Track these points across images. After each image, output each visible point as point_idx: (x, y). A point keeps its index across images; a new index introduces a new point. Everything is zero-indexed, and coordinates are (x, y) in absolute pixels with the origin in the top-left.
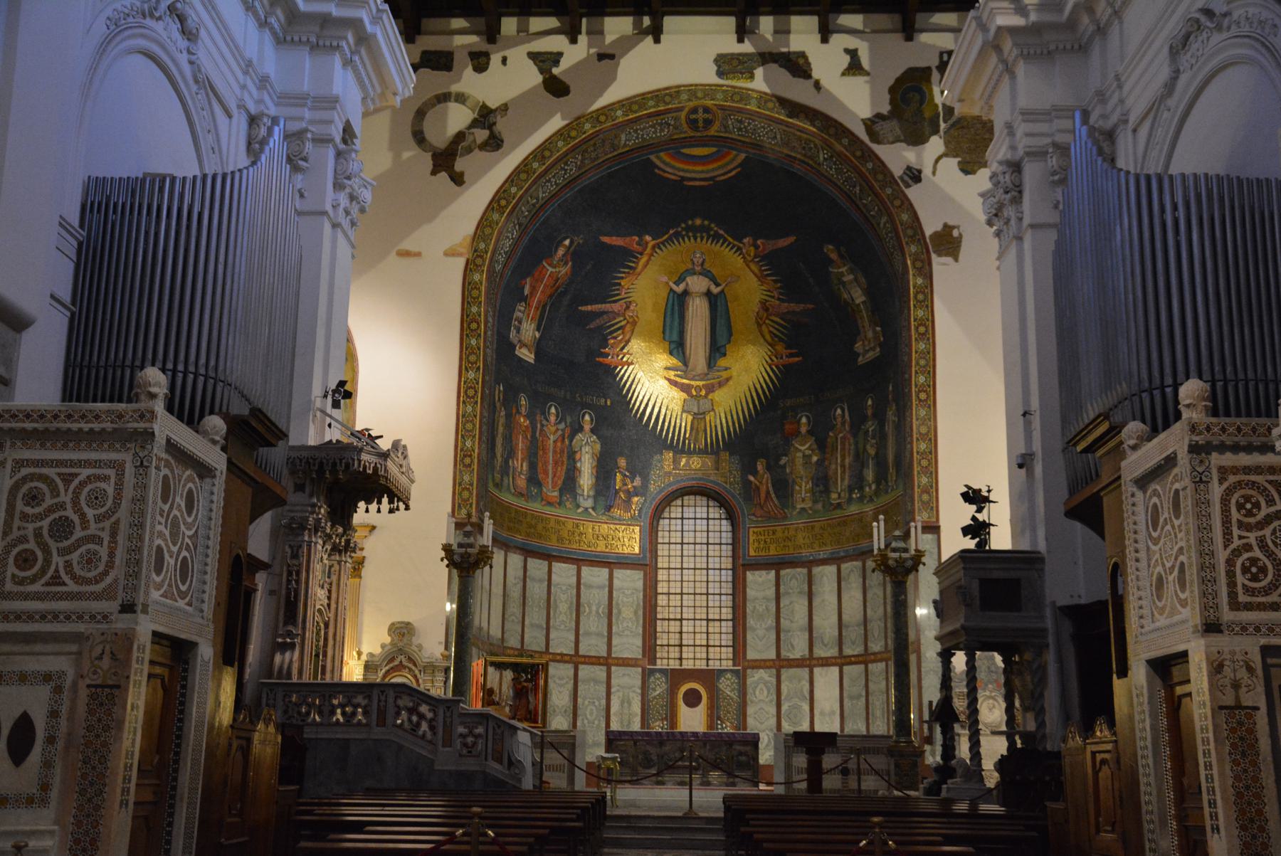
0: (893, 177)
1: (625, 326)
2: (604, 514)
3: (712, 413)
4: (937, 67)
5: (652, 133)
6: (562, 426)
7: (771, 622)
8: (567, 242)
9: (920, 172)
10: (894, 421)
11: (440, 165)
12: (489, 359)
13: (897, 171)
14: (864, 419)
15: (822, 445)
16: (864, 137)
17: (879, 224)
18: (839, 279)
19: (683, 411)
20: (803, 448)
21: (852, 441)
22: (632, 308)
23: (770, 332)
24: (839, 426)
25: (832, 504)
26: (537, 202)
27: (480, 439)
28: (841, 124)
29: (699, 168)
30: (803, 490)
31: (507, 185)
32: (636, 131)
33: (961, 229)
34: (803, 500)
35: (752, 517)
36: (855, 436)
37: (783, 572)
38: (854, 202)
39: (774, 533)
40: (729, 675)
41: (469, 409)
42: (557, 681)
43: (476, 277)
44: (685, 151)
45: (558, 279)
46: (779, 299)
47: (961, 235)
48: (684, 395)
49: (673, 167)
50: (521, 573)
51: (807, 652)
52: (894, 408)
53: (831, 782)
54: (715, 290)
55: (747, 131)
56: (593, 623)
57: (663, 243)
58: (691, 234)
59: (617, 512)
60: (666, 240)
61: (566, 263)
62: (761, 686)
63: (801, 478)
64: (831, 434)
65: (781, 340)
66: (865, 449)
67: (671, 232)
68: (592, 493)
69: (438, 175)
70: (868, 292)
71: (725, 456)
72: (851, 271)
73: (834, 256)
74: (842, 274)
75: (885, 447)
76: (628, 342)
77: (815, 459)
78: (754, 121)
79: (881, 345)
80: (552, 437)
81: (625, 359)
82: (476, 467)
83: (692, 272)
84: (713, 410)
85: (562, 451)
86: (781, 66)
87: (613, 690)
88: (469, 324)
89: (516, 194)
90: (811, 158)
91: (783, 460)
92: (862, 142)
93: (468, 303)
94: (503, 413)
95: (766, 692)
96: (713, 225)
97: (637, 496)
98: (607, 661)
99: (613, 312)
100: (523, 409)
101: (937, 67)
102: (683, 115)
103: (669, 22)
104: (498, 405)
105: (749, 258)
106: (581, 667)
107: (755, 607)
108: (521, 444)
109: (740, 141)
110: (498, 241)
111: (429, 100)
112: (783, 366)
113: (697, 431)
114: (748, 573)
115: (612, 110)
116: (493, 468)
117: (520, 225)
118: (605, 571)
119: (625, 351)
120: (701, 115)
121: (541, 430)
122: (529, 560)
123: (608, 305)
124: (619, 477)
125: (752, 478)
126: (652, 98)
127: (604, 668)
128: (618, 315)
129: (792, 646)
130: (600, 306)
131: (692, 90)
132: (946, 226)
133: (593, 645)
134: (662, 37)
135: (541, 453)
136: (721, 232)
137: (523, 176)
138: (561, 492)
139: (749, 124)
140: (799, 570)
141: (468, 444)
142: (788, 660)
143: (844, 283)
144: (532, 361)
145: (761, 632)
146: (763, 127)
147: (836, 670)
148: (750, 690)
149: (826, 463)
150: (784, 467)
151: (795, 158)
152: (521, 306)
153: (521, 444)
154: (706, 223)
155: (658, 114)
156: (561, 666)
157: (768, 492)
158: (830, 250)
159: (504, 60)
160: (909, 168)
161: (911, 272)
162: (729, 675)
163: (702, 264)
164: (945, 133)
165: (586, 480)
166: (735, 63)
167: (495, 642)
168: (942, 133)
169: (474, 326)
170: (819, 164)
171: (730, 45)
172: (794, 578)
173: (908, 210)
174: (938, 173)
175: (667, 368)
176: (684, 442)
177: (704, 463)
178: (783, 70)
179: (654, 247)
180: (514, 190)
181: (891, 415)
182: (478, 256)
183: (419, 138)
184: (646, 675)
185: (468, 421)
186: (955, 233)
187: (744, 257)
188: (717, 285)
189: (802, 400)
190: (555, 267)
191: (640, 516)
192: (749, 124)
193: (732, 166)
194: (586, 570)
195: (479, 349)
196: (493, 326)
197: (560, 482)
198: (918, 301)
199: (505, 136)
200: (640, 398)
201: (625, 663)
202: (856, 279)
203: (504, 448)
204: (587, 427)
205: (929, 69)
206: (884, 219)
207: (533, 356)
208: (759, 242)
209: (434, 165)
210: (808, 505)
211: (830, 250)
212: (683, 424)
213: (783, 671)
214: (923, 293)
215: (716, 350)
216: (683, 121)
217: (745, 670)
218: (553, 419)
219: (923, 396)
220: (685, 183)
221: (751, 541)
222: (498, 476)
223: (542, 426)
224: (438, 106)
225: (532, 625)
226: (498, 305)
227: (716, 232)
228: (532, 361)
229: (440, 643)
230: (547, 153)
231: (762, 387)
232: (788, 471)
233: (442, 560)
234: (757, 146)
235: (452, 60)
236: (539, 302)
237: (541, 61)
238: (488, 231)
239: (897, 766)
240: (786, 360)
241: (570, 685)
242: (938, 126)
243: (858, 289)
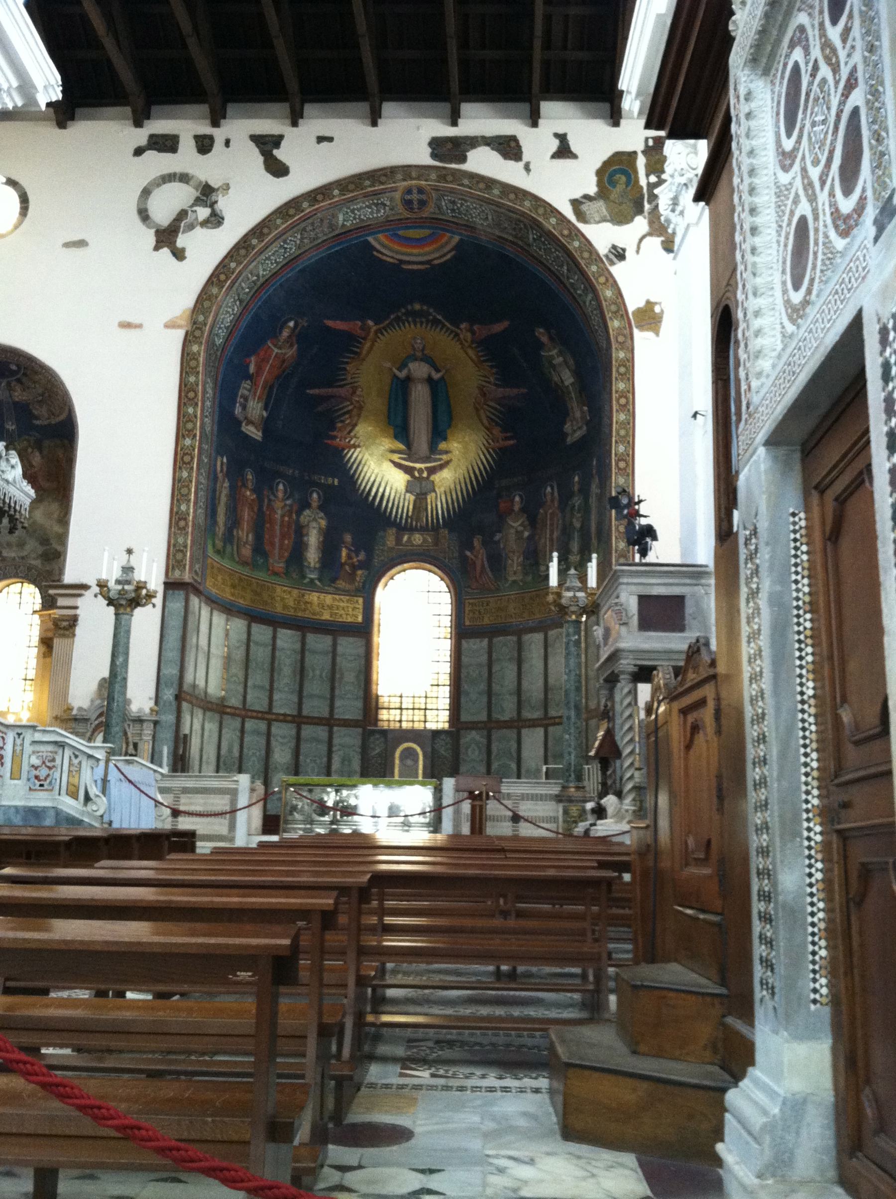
0: (598, 255)
1: (351, 410)
2: (330, 586)
3: (433, 494)
4: (643, 152)
5: (366, 212)
6: (288, 502)
7: (483, 686)
8: (291, 324)
9: (624, 250)
10: (597, 494)
11: (162, 241)
12: (208, 429)
13: (602, 248)
14: (571, 495)
15: (533, 521)
16: (572, 218)
17: (585, 303)
18: (550, 363)
19: (407, 491)
20: (516, 524)
21: (560, 515)
22: (358, 393)
23: (488, 417)
24: (549, 503)
25: (540, 576)
26: (258, 280)
27: (195, 503)
28: (550, 205)
29: (415, 251)
30: (515, 564)
31: (227, 261)
32: (353, 211)
33: (663, 305)
34: (515, 573)
35: (469, 590)
36: (563, 510)
37: (495, 640)
38: (562, 283)
39: (488, 605)
40: (443, 737)
41: (185, 474)
42: (281, 740)
43: (195, 348)
44: (401, 233)
45: (284, 361)
46: (496, 385)
47: (662, 311)
48: (407, 477)
49: (390, 250)
50: (245, 636)
51: (515, 714)
52: (597, 480)
53: (492, 830)
54: (436, 376)
55: (460, 213)
56: (315, 687)
57: (384, 328)
58: (410, 319)
59: (341, 584)
60: (388, 325)
61: (291, 346)
62: (473, 745)
63: (514, 552)
64: (541, 511)
65: (497, 424)
66: (571, 524)
67: (392, 317)
68: (317, 566)
69: (161, 251)
70: (578, 373)
71: (445, 532)
72: (560, 353)
73: (544, 339)
74: (552, 357)
75: (589, 520)
76: (355, 425)
77: (526, 534)
78: (466, 201)
79: (587, 423)
80: (279, 512)
81: (352, 442)
82: (190, 529)
83: (415, 358)
84: (434, 491)
85: (289, 527)
86: (493, 149)
87: (334, 749)
88: (188, 393)
89: (235, 269)
90: (521, 239)
91: (498, 537)
92: (569, 222)
93: (187, 373)
94: (226, 484)
95: (477, 753)
96: (431, 310)
97: (360, 568)
98: (330, 722)
99: (340, 397)
100: (250, 484)
101: (643, 152)
102: (397, 195)
103: (388, 108)
104: (220, 475)
105: (466, 344)
106: (304, 727)
107: (468, 673)
108: (246, 515)
109: (453, 222)
110: (217, 315)
111: (154, 179)
112: (500, 449)
113: (419, 512)
114: (464, 643)
115: (329, 189)
116: (214, 534)
117: (241, 301)
118: (328, 640)
119: (352, 434)
120: (415, 196)
121: (269, 505)
122: (253, 625)
123: (335, 390)
124: (344, 553)
125: (468, 553)
126: (368, 179)
127: (326, 728)
128: (346, 399)
129: (503, 710)
130: (326, 390)
131: (407, 170)
132: (648, 302)
133: (315, 707)
134: (379, 121)
135: (268, 525)
136: (439, 317)
137: (243, 252)
138: (288, 563)
139: (462, 205)
140: (509, 637)
141: (183, 507)
142: (498, 722)
143: (554, 367)
144: (259, 439)
145: (474, 696)
146: (475, 208)
147: (540, 731)
148: (462, 750)
149: (537, 537)
150: (499, 541)
151: (506, 240)
152: (246, 384)
153: (246, 515)
154: (425, 308)
155: (375, 194)
156: (283, 725)
157: (483, 566)
158: (541, 333)
159: (227, 143)
160: (614, 247)
161: (614, 347)
162: (443, 737)
163: (423, 350)
164: (649, 213)
165: (312, 556)
166: (449, 145)
167: (213, 700)
168: (646, 214)
169: (191, 395)
170: (529, 245)
171: (447, 131)
172: (505, 644)
173: (612, 286)
174: (641, 251)
175: (393, 451)
176: (406, 520)
177: (425, 540)
178: (495, 153)
179: (376, 332)
180: (233, 265)
181: (594, 489)
182: (197, 328)
183: (144, 215)
184: (367, 735)
185: (183, 486)
186: (657, 309)
187: (461, 344)
188: (438, 370)
189: (515, 480)
190: (280, 348)
191: (364, 587)
192: (462, 205)
193: (446, 250)
194: (311, 638)
195: (196, 417)
196: (214, 398)
197: (286, 554)
198: (620, 374)
199: (226, 214)
200: (367, 478)
201: (346, 723)
202: (565, 362)
203: (228, 518)
204: (315, 504)
205: (635, 153)
206: (590, 297)
207: (260, 434)
208: (475, 327)
209: (157, 242)
210: (519, 577)
211: (541, 333)
212: (406, 504)
213: (494, 731)
214: (625, 366)
215: (438, 434)
216: (399, 202)
217: (458, 731)
218: (280, 495)
219: (622, 465)
220: (405, 267)
221: (467, 612)
222: (219, 544)
223: (270, 500)
224: (164, 186)
225: (255, 686)
226: (219, 379)
227: (435, 317)
228: (259, 439)
229: (150, 699)
230: (266, 231)
231: (479, 468)
232: (502, 546)
233: (96, 596)
234: (471, 227)
235: (178, 143)
236: (266, 382)
237: (262, 144)
238: (207, 304)
239: (566, 812)
240: (502, 444)
241: (293, 744)
242: (642, 206)
243: (567, 371)
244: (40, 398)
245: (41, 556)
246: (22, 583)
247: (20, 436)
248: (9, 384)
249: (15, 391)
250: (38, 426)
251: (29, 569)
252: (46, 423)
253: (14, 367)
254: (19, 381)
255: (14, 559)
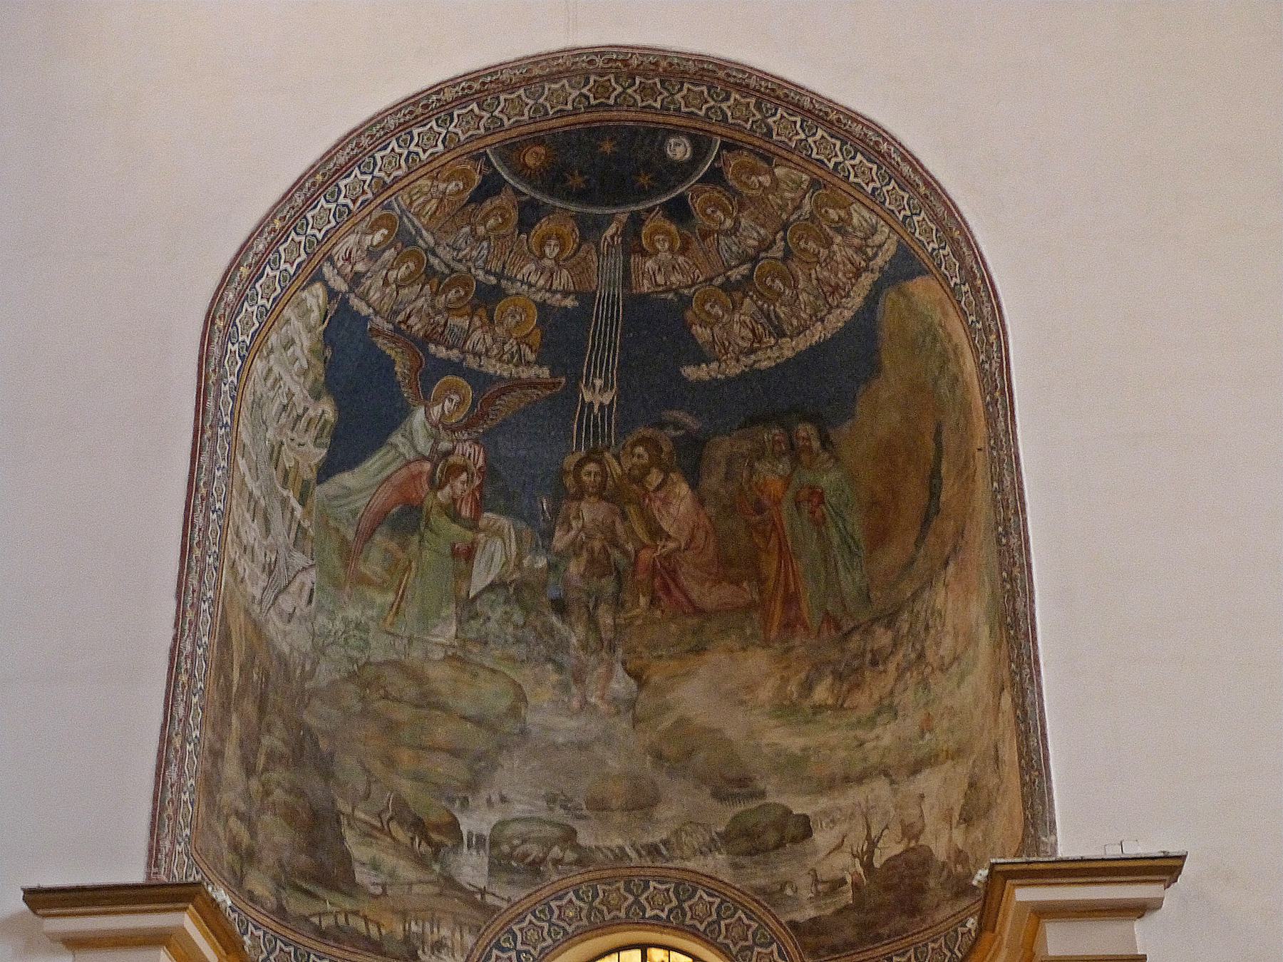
244: (735, 275)
245: (726, 838)
246: (644, 947)
247: (625, 427)
248: (636, 221)
249: (644, 253)
250: (699, 382)
251: (686, 886)
252: (734, 370)
253: (679, 150)
254: (679, 211)
255: (621, 855)
